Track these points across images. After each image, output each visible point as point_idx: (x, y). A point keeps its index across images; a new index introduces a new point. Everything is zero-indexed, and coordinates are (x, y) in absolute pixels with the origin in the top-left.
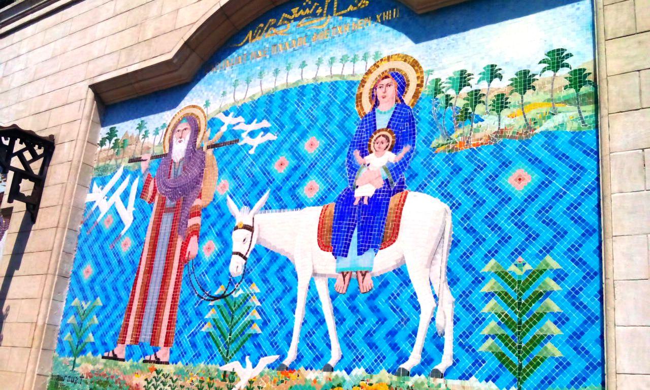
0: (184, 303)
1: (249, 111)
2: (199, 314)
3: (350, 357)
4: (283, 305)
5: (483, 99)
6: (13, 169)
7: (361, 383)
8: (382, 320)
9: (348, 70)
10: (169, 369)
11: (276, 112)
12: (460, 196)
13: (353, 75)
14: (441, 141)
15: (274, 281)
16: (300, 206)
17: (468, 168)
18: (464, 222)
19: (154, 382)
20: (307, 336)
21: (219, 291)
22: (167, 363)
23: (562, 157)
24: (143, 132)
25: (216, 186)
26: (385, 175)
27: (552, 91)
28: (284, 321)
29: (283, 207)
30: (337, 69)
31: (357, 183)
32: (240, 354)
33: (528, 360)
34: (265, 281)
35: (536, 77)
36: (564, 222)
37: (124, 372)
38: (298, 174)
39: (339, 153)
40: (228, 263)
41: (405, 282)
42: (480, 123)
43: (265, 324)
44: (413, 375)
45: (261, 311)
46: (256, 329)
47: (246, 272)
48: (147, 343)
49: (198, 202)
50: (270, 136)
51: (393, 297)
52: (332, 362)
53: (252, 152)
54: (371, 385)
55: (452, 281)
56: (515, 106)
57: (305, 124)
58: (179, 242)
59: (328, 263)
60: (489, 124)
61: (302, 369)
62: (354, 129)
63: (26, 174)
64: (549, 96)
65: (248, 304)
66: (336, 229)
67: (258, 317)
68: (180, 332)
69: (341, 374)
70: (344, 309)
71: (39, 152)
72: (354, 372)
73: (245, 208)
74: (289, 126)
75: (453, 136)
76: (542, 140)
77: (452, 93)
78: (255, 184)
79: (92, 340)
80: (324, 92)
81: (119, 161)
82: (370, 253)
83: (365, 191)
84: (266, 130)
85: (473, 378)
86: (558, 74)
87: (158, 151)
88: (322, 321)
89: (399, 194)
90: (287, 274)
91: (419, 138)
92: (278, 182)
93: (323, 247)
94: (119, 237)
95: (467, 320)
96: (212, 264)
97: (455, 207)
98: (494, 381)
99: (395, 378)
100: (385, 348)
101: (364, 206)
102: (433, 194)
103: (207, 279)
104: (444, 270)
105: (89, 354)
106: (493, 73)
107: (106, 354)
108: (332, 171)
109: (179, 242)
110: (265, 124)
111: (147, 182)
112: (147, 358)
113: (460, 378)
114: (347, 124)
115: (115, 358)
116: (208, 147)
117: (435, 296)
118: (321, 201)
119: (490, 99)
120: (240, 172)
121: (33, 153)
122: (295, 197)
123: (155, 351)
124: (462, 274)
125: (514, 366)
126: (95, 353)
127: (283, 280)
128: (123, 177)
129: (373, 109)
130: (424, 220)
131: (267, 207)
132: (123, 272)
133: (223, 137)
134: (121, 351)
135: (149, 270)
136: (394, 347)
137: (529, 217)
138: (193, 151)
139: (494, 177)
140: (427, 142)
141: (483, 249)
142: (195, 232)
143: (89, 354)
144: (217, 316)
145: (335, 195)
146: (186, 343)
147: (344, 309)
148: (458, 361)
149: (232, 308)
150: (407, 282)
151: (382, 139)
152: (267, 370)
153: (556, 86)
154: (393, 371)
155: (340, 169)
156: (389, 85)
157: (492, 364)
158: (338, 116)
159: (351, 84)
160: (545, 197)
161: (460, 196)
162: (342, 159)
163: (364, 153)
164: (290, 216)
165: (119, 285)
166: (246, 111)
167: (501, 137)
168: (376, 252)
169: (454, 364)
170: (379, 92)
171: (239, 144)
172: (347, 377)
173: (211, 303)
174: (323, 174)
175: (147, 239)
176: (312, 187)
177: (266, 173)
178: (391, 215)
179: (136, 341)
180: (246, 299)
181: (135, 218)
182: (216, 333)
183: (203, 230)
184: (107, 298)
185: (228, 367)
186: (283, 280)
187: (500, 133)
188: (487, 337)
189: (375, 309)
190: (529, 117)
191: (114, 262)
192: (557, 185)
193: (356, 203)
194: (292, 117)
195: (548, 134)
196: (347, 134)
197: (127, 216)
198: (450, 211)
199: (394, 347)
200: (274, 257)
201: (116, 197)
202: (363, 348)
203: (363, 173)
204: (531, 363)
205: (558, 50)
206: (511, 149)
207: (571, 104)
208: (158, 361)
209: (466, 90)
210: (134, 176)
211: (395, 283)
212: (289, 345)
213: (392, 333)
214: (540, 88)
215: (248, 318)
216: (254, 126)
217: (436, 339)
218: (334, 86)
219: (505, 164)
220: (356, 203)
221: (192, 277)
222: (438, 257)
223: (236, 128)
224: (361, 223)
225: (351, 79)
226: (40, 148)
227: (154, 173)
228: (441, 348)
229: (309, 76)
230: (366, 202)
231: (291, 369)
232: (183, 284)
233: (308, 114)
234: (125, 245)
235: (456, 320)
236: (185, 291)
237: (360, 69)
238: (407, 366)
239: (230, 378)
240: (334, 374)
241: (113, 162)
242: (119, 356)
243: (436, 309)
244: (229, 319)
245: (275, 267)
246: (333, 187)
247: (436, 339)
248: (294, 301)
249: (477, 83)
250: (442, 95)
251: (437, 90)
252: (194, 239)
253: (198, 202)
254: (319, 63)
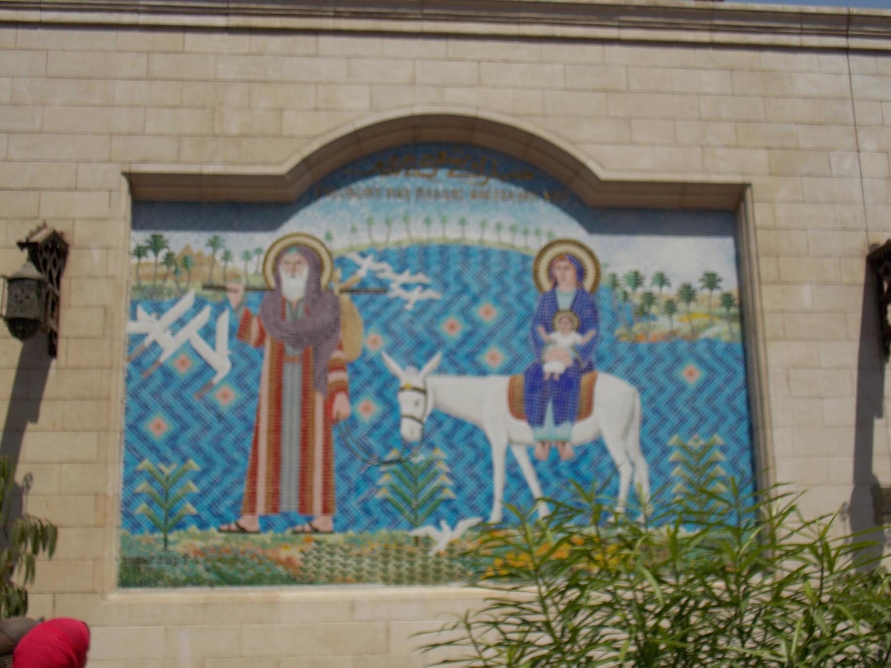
2: (367, 479)
9: (520, 242)
15: (463, 447)
18: (650, 402)
21: (393, 455)
23: (720, 360)
28: (481, 486)
30: (506, 238)
34: (452, 446)
36: (724, 410)
38: (475, 340)
39: (520, 326)
40: (397, 425)
43: (459, 489)
45: (451, 476)
46: (449, 493)
49: (337, 354)
57: (475, 288)
58: (319, 400)
59: (523, 431)
62: (536, 305)
65: (433, 470)
66: (529, 401)
67: (449, 482)
70: (548, 474)
73: (411, 370)
74: (454, 288)
76: (705, 345)
80: (494, 259)
90: (477, 439)
92: (451, 345)
96: (376, 426)
103: (372, 442)
108: (515, 343)
109: (319, 400)
122: (475, 364)
124: (651, 444)
127: (474, 446)
130: (613, 400)
135: (277, 429)
137: (700, 403)
141: (668, 426)
144: (395, 481)
147: (548, 474)
155: (524, 342)
158: (515, 289)
159: (525, 258)
160: (711, 389)
164: (471, 383)
170: (558, 273)
174: (505, 344)
176: (494, 355)
180: (430, 464)
181: (234, 364)
182: (396, 499)
183: (351, 389)
186: (474, 446)
192: (718, 381)
193: (547, 377)
194: (458, 276)
196: (528, 308)
200: (459, 423)
206: (682, 347)
215: (436, 484)
220: (547, 377)
221: (348, 439)
224: (551, 396)
229: (473, 236)
233: (478, 278)
234: (226, 397)
236: (340, 456)
237: (534, 244)
246: (517, 359)
248: (490, 467)
254: (483, 225)
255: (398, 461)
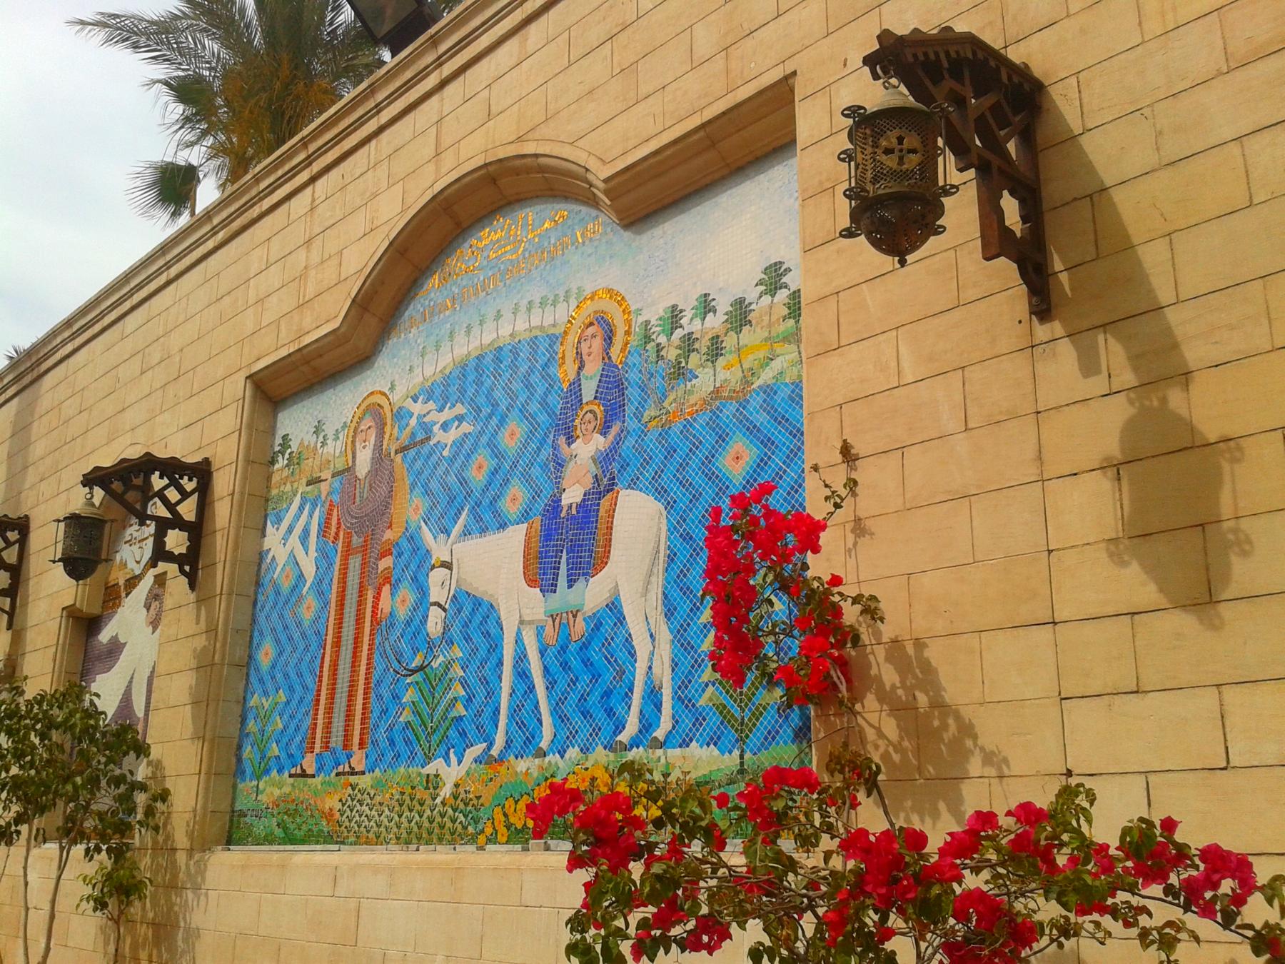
0: (379, 683)
1: (440, 392)
2: (396, 697)
3: (564, 733)
4: (487, 671)
5: (696, 346)
6: (153, 518)
7: (576, 769)
8: (596, 677)
10: (365, 781)
11: (470, 391)
12: (676, 491)
13: (554, 326)
14: (653, 414)
15: (477, 638)
16: (503, 526)
17: (683, 448)
19: (350, 802)
20: (515, 711)
22: (363, 773)
24: (321, 439)
25: (411, 509)
26: (593, 469)
27: (770, 325)
29: (483, 531)
31: (565, 484)
32: (443, 748)
33: (750, 710)
34: (468, 639)
35: (753, 307)
37: (316, 793)
39: (543, 442)
40: (425, 618)
41: (619, 620)
42: (694, 381)
44: (632, 747)
45: (464, 684)
46: (460, 710)
47: (446, 629)
48: (340, 746)
49: (388, 535)
50: (466, 427)
51: (607, 643)
52: (544, 744)
53: (446, 453)
54: (587, 769)
55: (669, 613)
56: (731, 352)
58: (370, 595)
59: (534, 604)
60: (704, 381)
61: (512, 758)
63: (176, 522)
64: (766, 334)
65: (450, 676)
68: (377, 726)
69: (553, 758)
70: (555, 668)
71: (189, 485)
72: (567, 756)
75: (666, 404)
77: (662, 339)
78: (452, 499)
79: (277, 753)
81: (295, 485)
82: (580, 584)
83: (572, 496)
84: (460, 418)
85: (694, 743)
86: (776, 300)
87: (340, 465)
88: (532, 688)
89: (609, 496)
91: (630, 410)
93: (531, 582)
94: (300, 598)
95: (686, 662)
96: (408, 623)
97: (670, 506)
98: (715, 744)
99: (611, 755)
100: (600, 715)
101: (573, 517)
102: (645, 490)
103: (404, 646)
104: (660, 595)
105: (274, 773)
106: (706, 306)
107: (293, 771)
108: (536, 471)
109: (370, 595)
110: (460, 409)
111: (330, 513)
112: (340, 769)
113: (681, 746)
114: (550, 399)
115: (304, 774)
116: (396, 452)
117: (651, 636)
118: (525, 516)
119: (703, 345)
120: (434, 485)
121: (180, 489)
122: (497, 514)
123: (349, 757)
125: (736, 720)
126: (280, 771)
127: (487, 635)
128: (301, 509)
129: (579, 374)
131: (466, 533)
132: (307, 648)
133: (413, 434)
134: (309, 764)
135: (337, 643)
136: (610, 712)
138: (380, 457)
139: (710, 458)
140: (638, 416)
142: (387, 580)
143: (274, 773)
145: (540, 506)
146: (384, 744)
148: (677, 722)
149: (432, 682)
150: (621, 620)
151: (589, 416)
152: (474, 765)
153: (774, 318)
154: (609, 747)
155: (544, 466)
156: (594, 336)
157: (714, 720)
159: (553, 339)
161: (676, 491)
162: (546, 452)
163: (570, 440)
164: (493, 540)
165: (304, 667)
166: (437, 392)
167: (716, 399)
168: (587, 581)
169: (674, 727)
171: (431, 443)
172: (561, 763)
173: (409, 680)
175: (333, 597)
176: (515, 497)
177: (463, 482)
178: (602, 526)
179: (326, 747)
180: (447, 667)
184: (291, 689)
185: (430, 769)
186: (487, 635)
187: (716, 393)
188: (707, 685)
189: (587, 663)
190: (746, 366)
191: (296, 636)
194: (489, 395)
195: (769, 391)
197: (309, 570)
198: (665, 513)
199: (610, 712)
200: (477, 602)
201: (294, 540)
202: (577, 720)
203: (570, 469)
204: (754, 714)
205: (776, 264)
207: (790, 342)
208: (353, 773)
209: (679, 333)
210: (314, 505)
211: (609, 623)
212: (497, 727)
213: (607, 694)
214: (758, 323)
216: (447, 414)
217: (653, 695)
218: (533, 342)
219: (722, 439)
222: (654, 579)
223: (425, 420)
224: (568, 543)
225: (552, 331)
226: (190, 480)
227: (336, 498)
228: (658, 706)
230: (574, 512)
231: (500, 760)
232: (376, 656)
234: (308, 609)
235: (675, 665)
238: (624, 737)
239: (433, 782)
240: (547, 759)
241: (288, 488)
242: (309, 771)
243: (652, 653)
244: (430, 701)
245: (478, 618)
247: (653, 695)
249: (690, 324)
250: (652, 344)
251: (647, 338)
252: (386, 589)
253: (388, 535)
255: (421, 668)
